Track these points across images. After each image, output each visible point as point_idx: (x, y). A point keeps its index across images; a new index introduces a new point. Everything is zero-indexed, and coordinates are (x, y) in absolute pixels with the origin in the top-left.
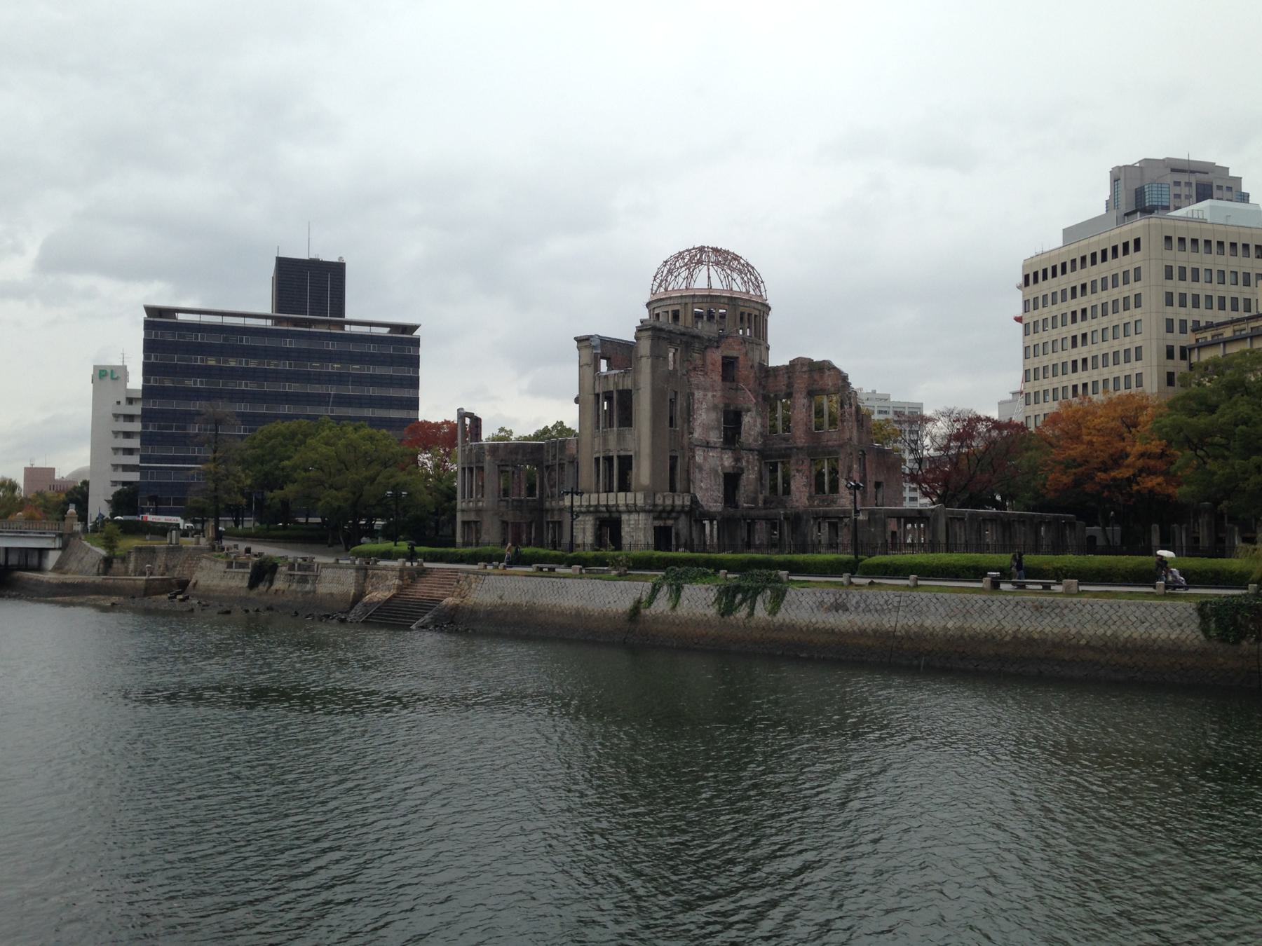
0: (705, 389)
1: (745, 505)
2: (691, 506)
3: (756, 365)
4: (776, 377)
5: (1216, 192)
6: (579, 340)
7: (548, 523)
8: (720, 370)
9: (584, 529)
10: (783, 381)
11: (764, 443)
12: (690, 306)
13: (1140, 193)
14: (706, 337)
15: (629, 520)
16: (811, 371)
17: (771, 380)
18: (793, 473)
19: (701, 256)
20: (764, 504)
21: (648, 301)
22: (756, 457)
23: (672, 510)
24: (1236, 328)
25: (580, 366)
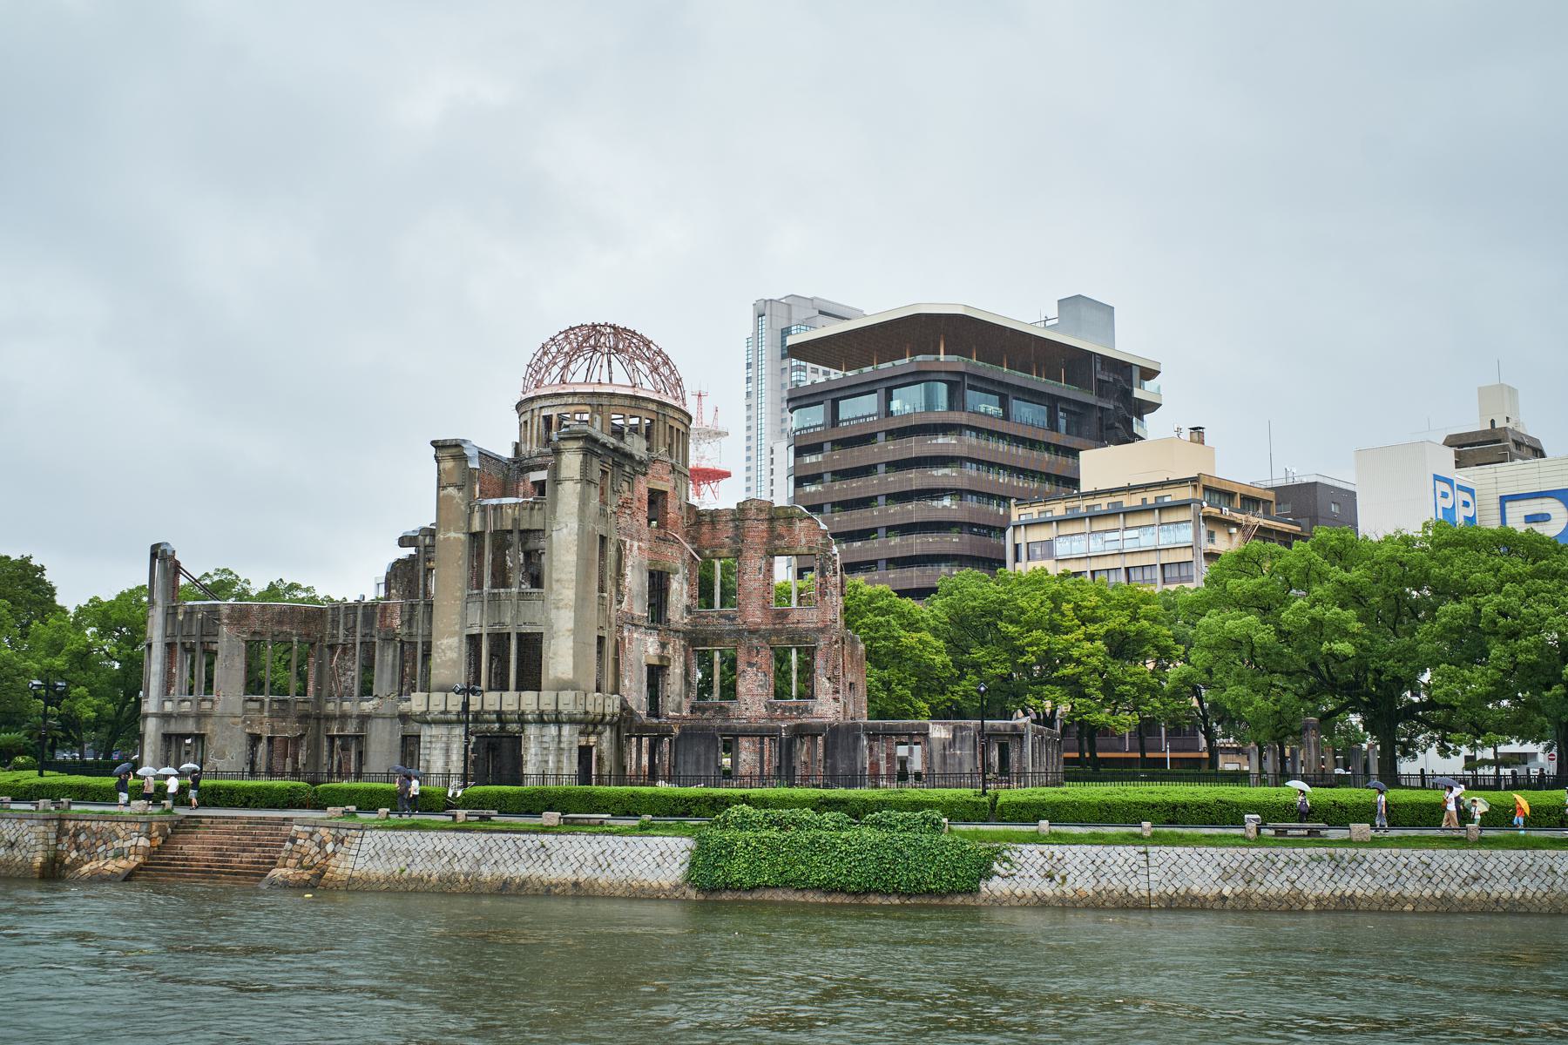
0: (632, 538)
1: (671, 714)
3: (684, 506)
4: (713, 523)
7: (332, 738)
10: (725, 533)
11: (694, 623)
14: (637, 458)
16: (771, 520)
17: (705, 529)
18: (741, 666)
20: (692, 712)
21: (519, 397)
22: (682, 643)
23: (602, 721)
24: (1069, 505)
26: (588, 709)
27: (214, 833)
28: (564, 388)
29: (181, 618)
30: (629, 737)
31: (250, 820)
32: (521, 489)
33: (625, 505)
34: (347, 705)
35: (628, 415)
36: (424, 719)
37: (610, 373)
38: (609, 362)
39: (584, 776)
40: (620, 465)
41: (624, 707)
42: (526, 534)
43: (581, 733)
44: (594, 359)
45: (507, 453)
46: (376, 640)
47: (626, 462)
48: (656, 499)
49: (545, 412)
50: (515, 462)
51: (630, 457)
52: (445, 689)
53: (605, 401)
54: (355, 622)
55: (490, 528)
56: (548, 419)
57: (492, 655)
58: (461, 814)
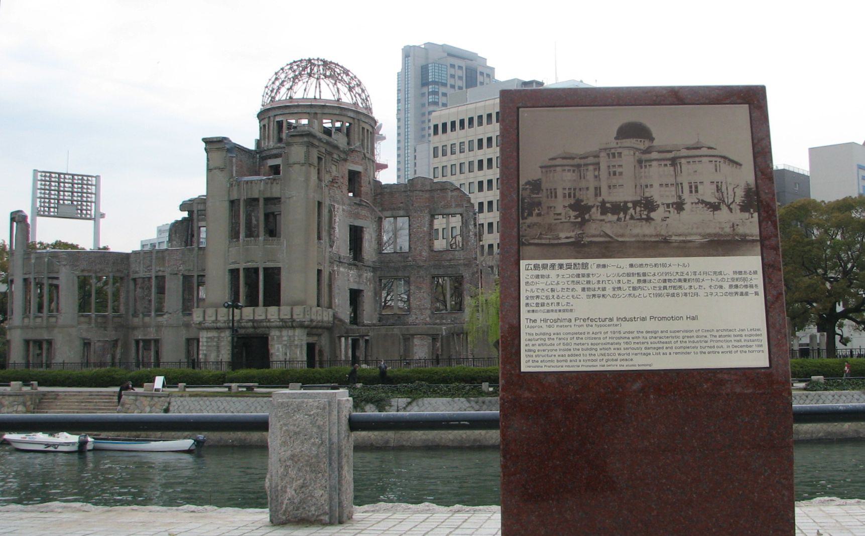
0: (338, 204)
2: (334, 322)
5: (480, 79)
6: (208, 142)
7: (137, 342)
8: (347, 184)
9: (218, 347)
12: (319, 116)
13: (424, 70)
14: (341, 149)
15: (281, 336)
19: (312, 70)
20: (379, 321)
21: (258, 108)
22: (372, 274)
25: (209, 170)
26: (314, 317)
27: (67, 402)
28: (291, 102)
29: (33, 261)
30: (340, 337)
31: (91, 394)
32: (262, 171)
33: (333, 181)
34: (147, 319)
35: (334, 120)
36: (201, 327)
37: (320, 92)
38: (320, 84)
39: (311, 362)
40: (330, 154)
41: (335, 317)
42: (268, 200)
43: (309, 335)
44: (309, 83)
45: (252, 146)
46: (165, 274)
47: (335, 151)
48: (354, 178)
49: (278, 119)
50: (257, 153)
51: (336, 147)
52: (216, 306)
53: (319, 111)
54: (151, 262)
55: (243, 197)
56: (280, 124)
57: (247, 283)
58: (234, 385)
